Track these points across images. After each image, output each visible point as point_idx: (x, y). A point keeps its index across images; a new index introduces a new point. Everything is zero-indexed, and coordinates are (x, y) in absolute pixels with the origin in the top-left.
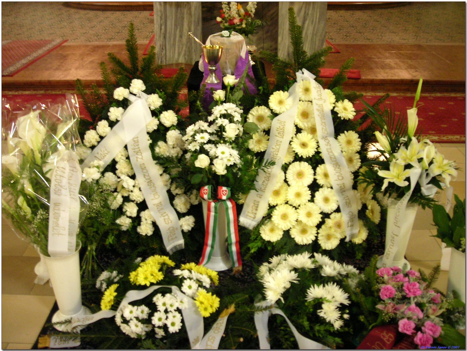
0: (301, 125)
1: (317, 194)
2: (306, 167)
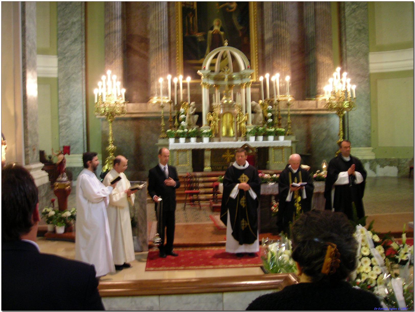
0: (363, 245)
1: (373, 268)
2: (367, 259)
